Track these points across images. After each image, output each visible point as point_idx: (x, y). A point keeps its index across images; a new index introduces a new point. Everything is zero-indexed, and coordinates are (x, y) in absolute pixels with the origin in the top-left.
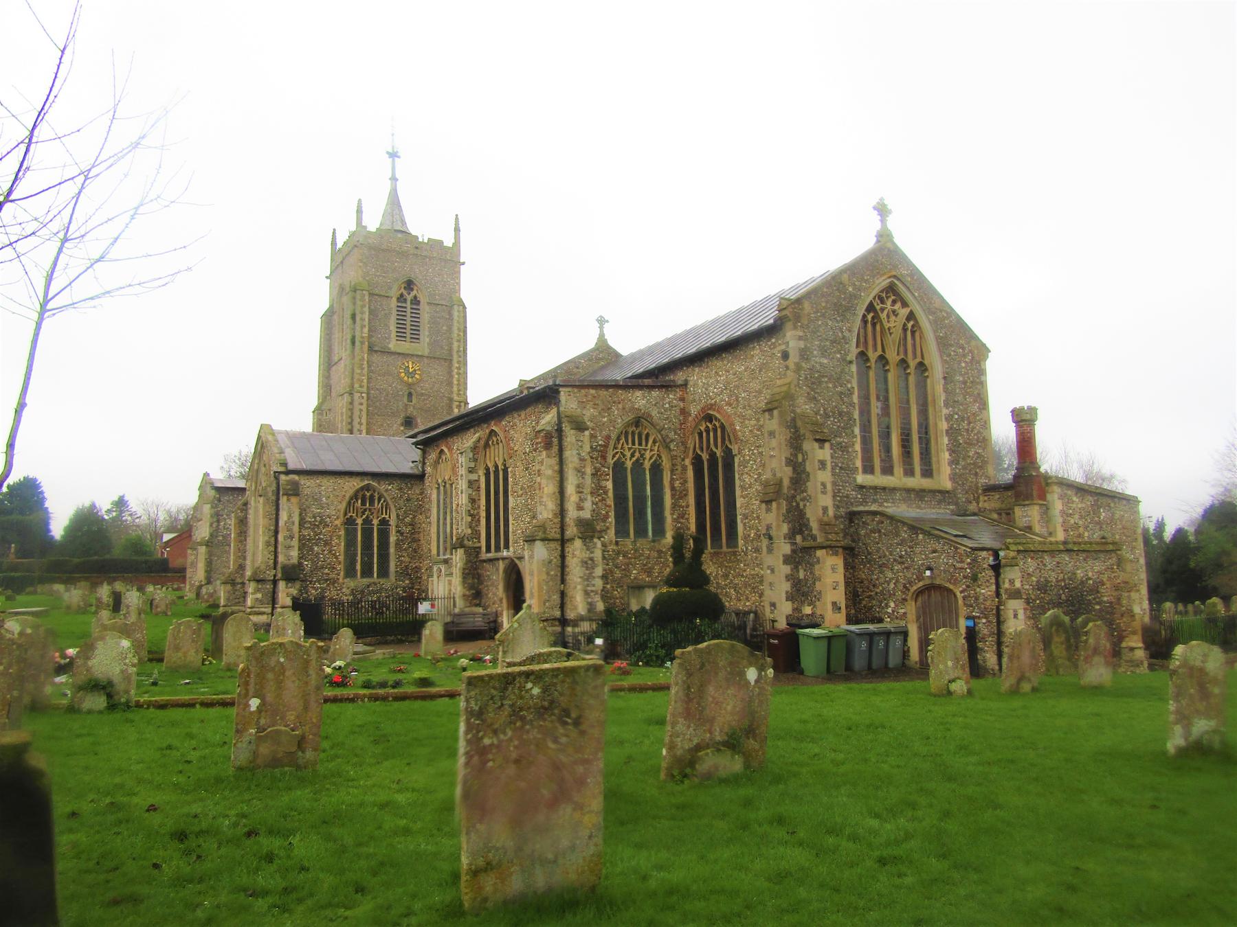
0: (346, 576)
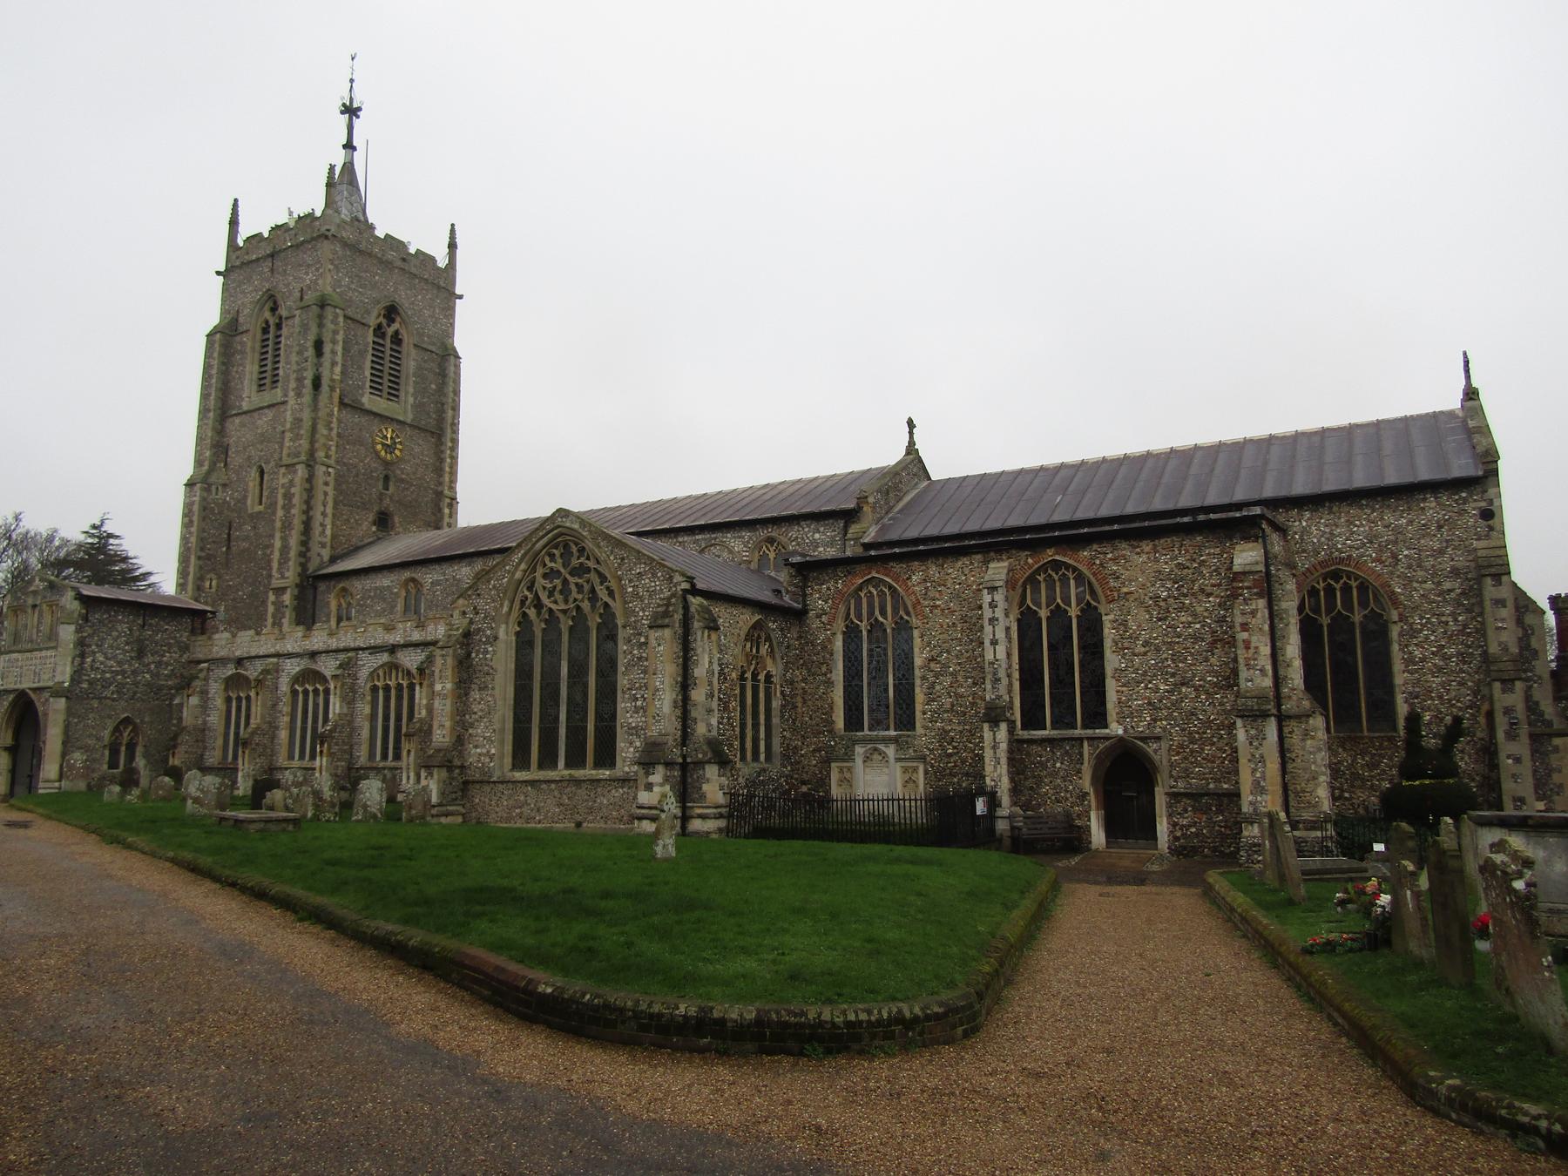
0: (741, 760)
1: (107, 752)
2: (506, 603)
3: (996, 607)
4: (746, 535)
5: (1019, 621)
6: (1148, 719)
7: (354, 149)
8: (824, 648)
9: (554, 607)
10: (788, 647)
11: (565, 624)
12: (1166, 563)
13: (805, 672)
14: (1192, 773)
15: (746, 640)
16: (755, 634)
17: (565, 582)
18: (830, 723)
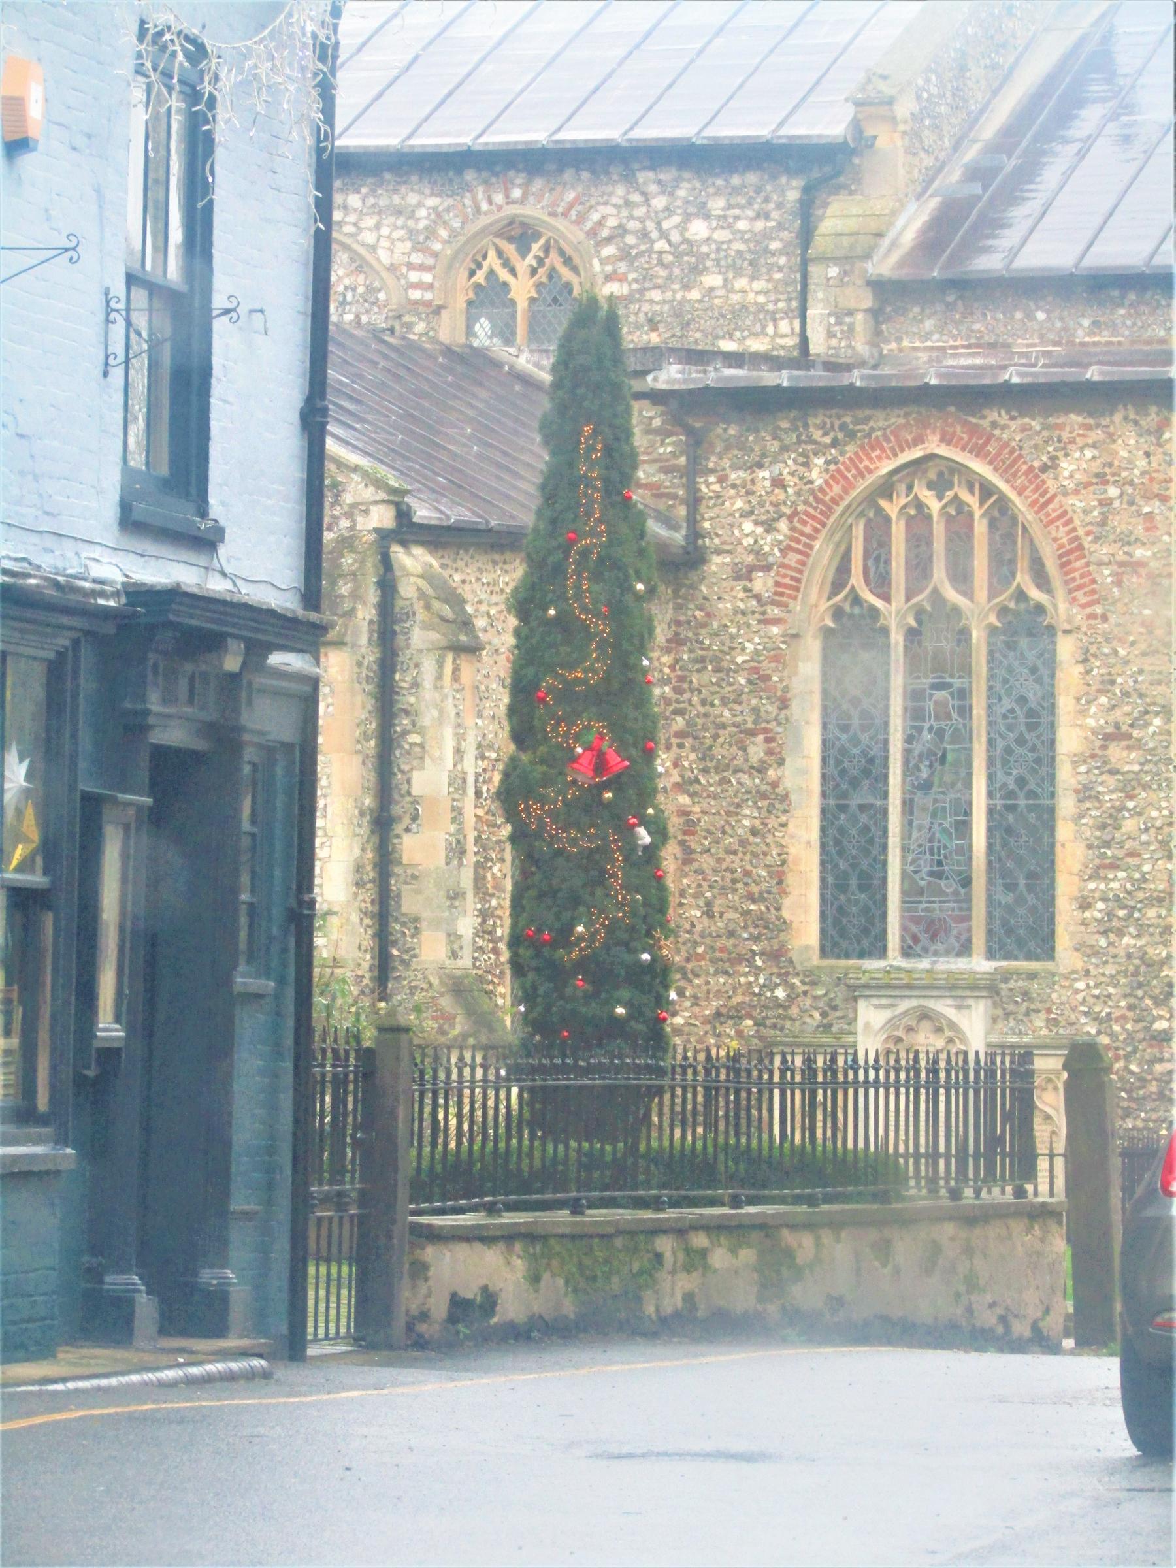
8: (759, 679)
13: (690, 759)
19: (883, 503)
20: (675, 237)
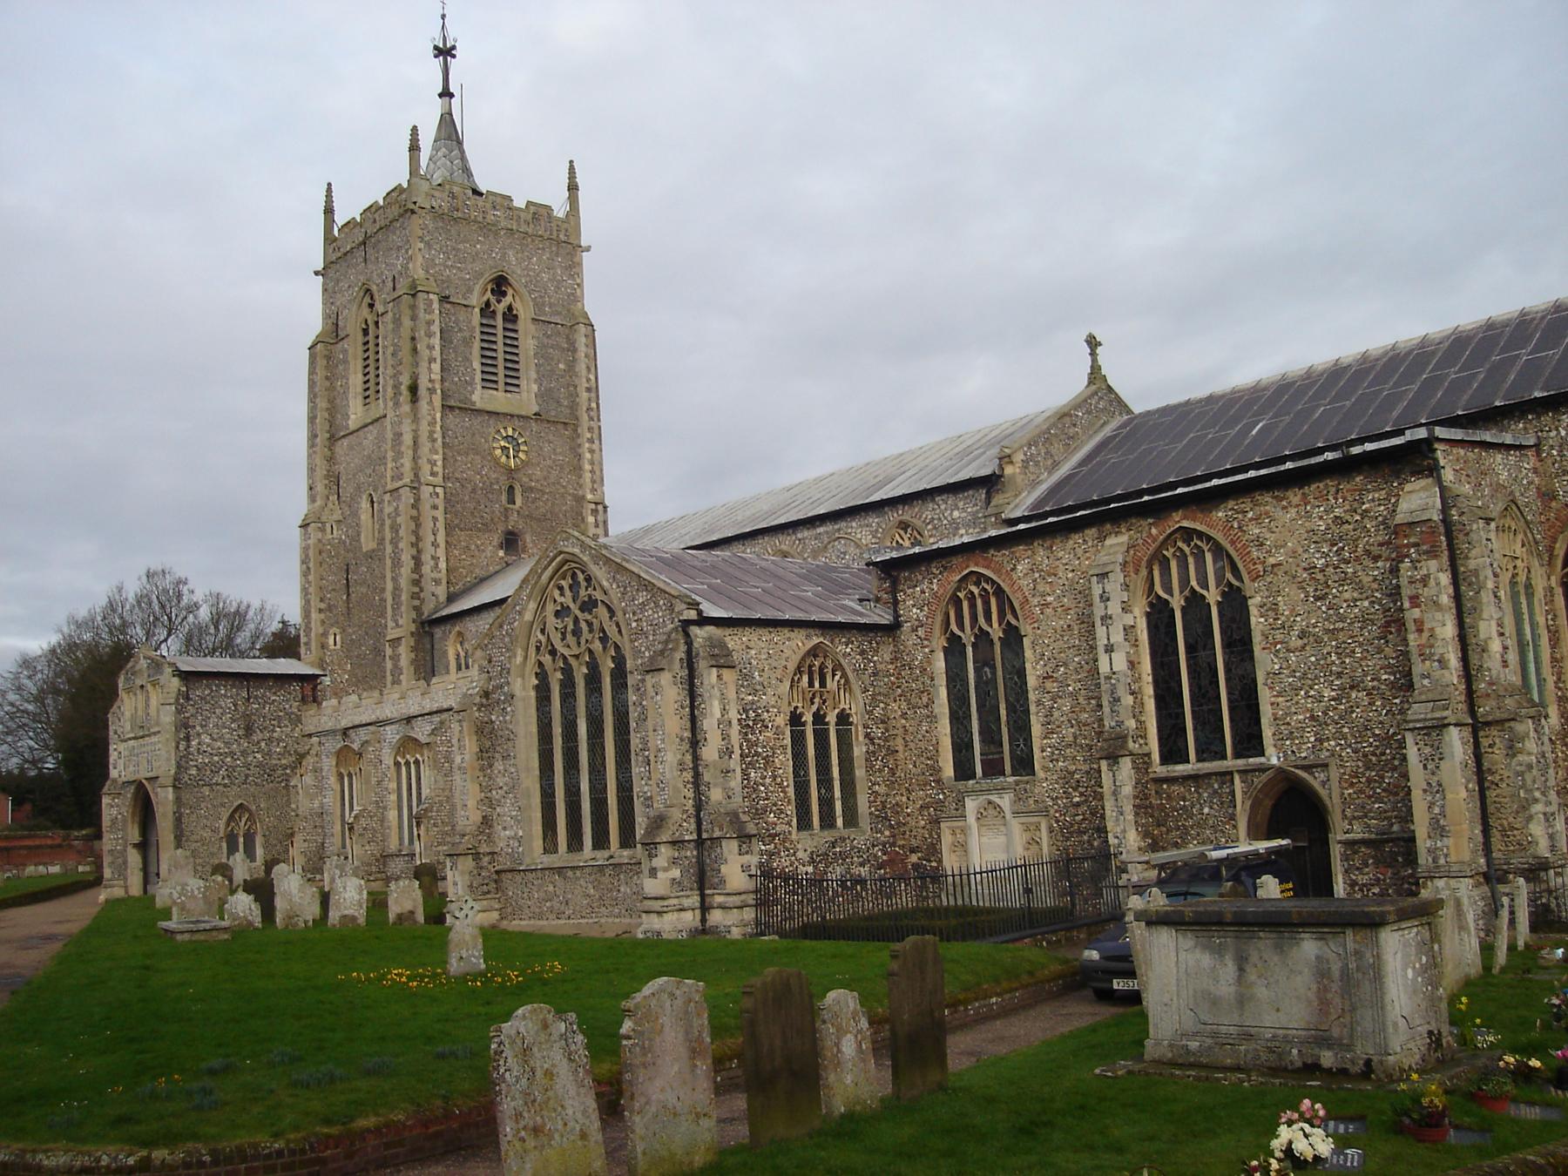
0: (799, 828)
1: (224, 845)
2: (520, 652)
3: (1108, 599)
4: (874, 520)
5: (1148, 615)
6: (1312, 739)
7: (451, 95)
9: (566, 652)
10: (875, 674)
11: (580, 672)
12: (1321, 518)
13: (904, 705)
14: (1371, 811)
15: (799, 670)
16: (813, 668)
17: (576, 620)
18: (936, 770)
19: (959, 594)
20: (949, 519)
